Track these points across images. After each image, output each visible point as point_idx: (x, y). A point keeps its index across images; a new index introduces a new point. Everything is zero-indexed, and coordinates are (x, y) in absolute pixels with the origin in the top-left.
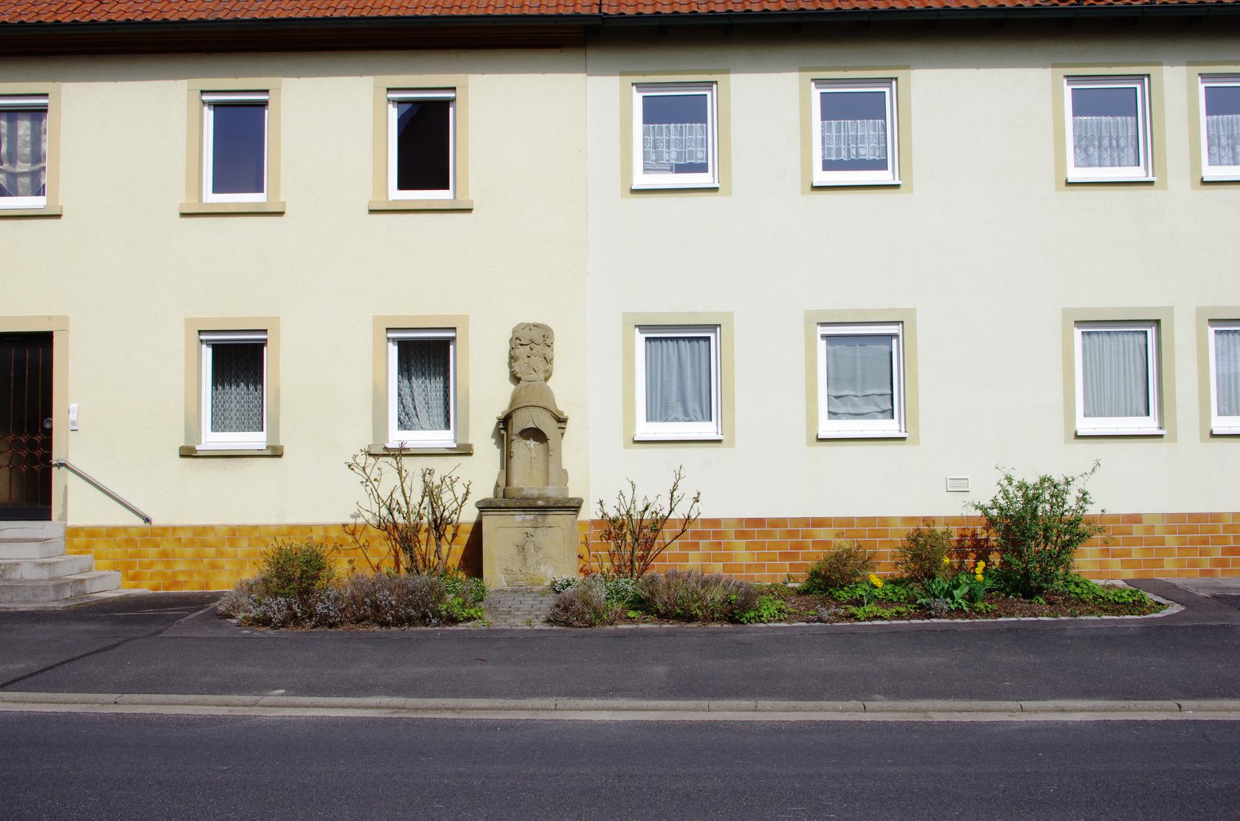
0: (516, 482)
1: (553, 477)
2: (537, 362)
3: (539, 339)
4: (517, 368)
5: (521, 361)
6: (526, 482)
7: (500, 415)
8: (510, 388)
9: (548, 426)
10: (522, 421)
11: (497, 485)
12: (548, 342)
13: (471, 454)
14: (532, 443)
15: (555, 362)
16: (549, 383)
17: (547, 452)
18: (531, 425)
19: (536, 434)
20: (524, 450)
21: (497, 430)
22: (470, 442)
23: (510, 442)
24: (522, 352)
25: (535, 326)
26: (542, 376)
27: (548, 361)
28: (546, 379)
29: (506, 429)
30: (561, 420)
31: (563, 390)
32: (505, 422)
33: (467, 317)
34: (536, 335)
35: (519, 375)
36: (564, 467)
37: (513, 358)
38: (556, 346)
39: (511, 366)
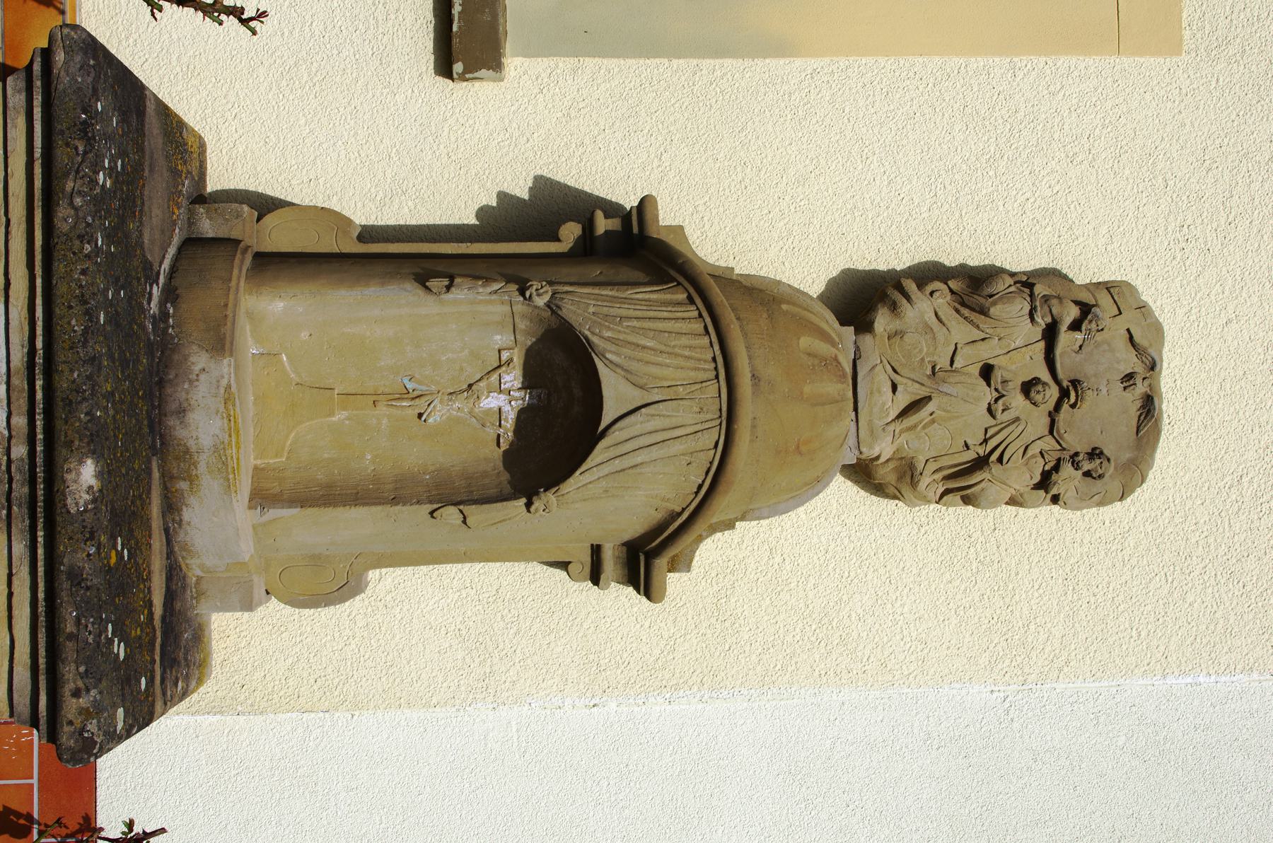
0: (275, 319)
1: (308, 530)
2: (960, 420)
3: (1081, 427)
4: (924, 307)
5: (960, 331)
6: (269, 381)
7: (667, 216)
8: (810, 275)
9: (612, 493)
10: (642, 351)
11: (265, 205)
12: (1068, 479)
13: (444, 67)
14: (504, 400)
15: (957, 515)
16: (841, 490)
17: (453, 494)
18: (616, 393)
19: (558, 430)
20: (470, 360)
21: (582, 206)
22: (513, 64)
23: (516, 273)
24: (1014, 339)
25: (1149, 406)
26: (883, 449)
27: (964, 480)
28: (862, 473)
29: (588, 248)
30: (642, 561)
31: (813, 562)
32: (632, 247)
33: (1173, 46)
34: (1103, 415)
35: (882, 321)
36: (382, 581)
37: (974, 287)
38: (1044, 515)
39: (928, 274)
